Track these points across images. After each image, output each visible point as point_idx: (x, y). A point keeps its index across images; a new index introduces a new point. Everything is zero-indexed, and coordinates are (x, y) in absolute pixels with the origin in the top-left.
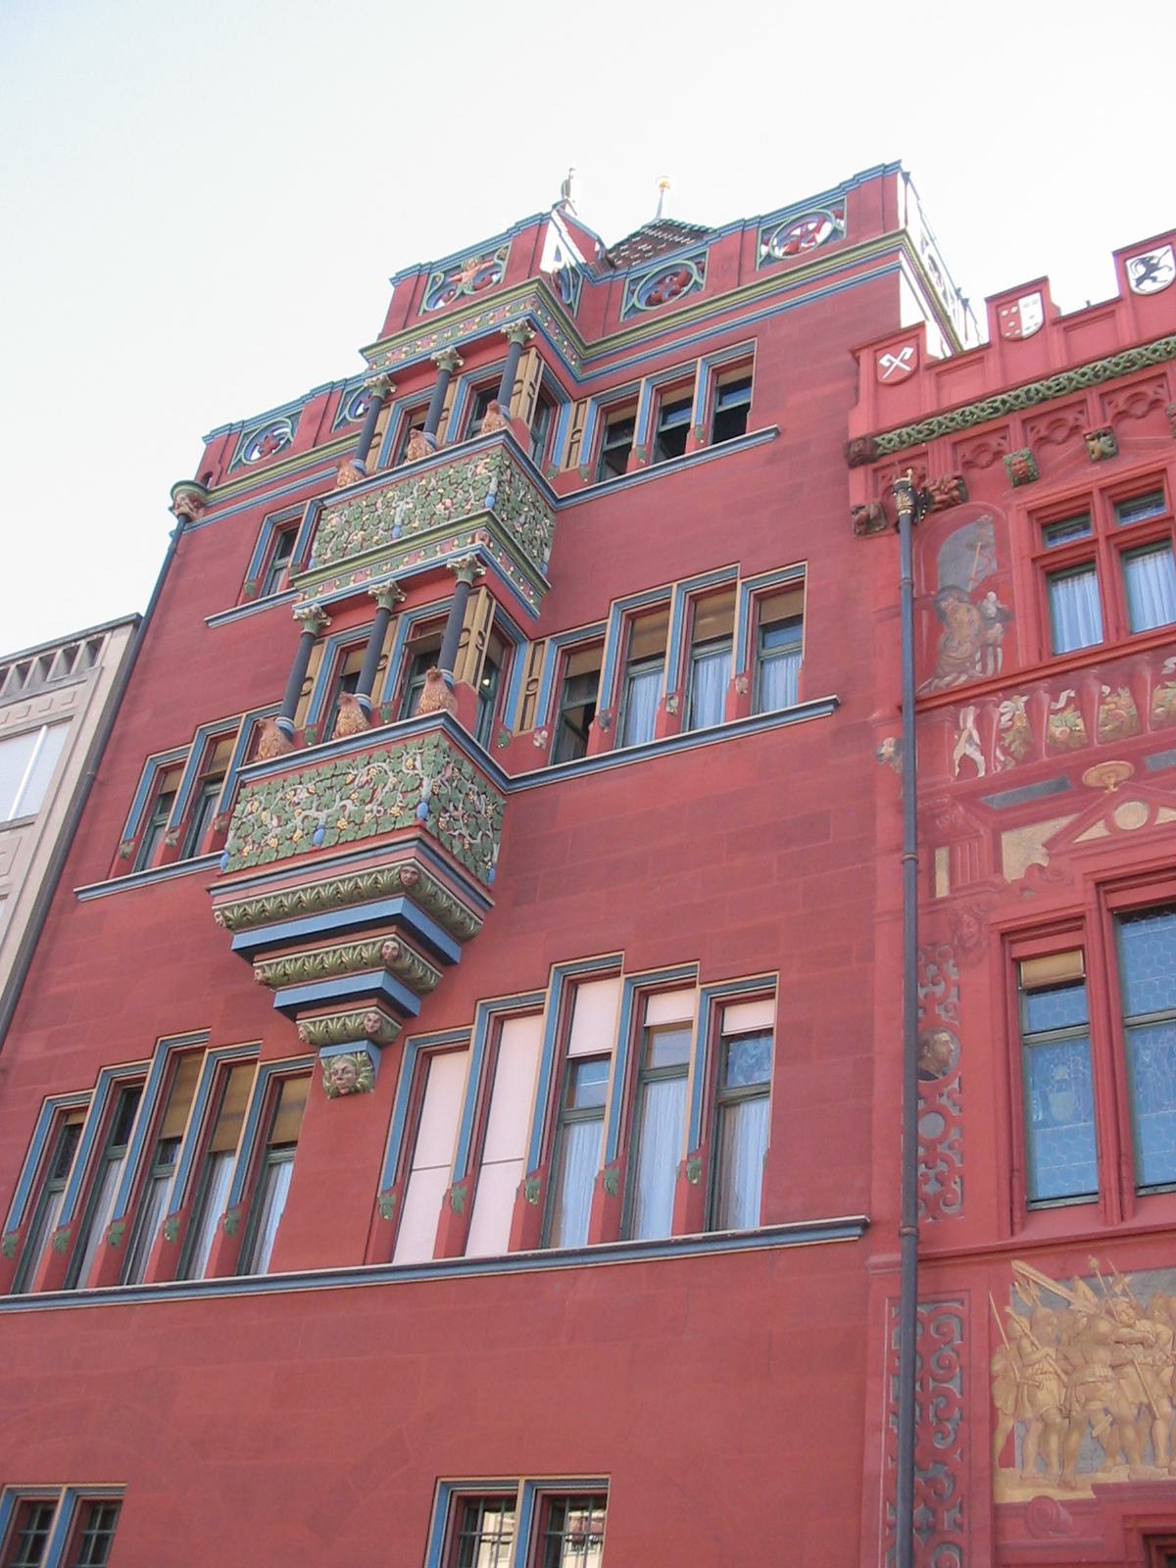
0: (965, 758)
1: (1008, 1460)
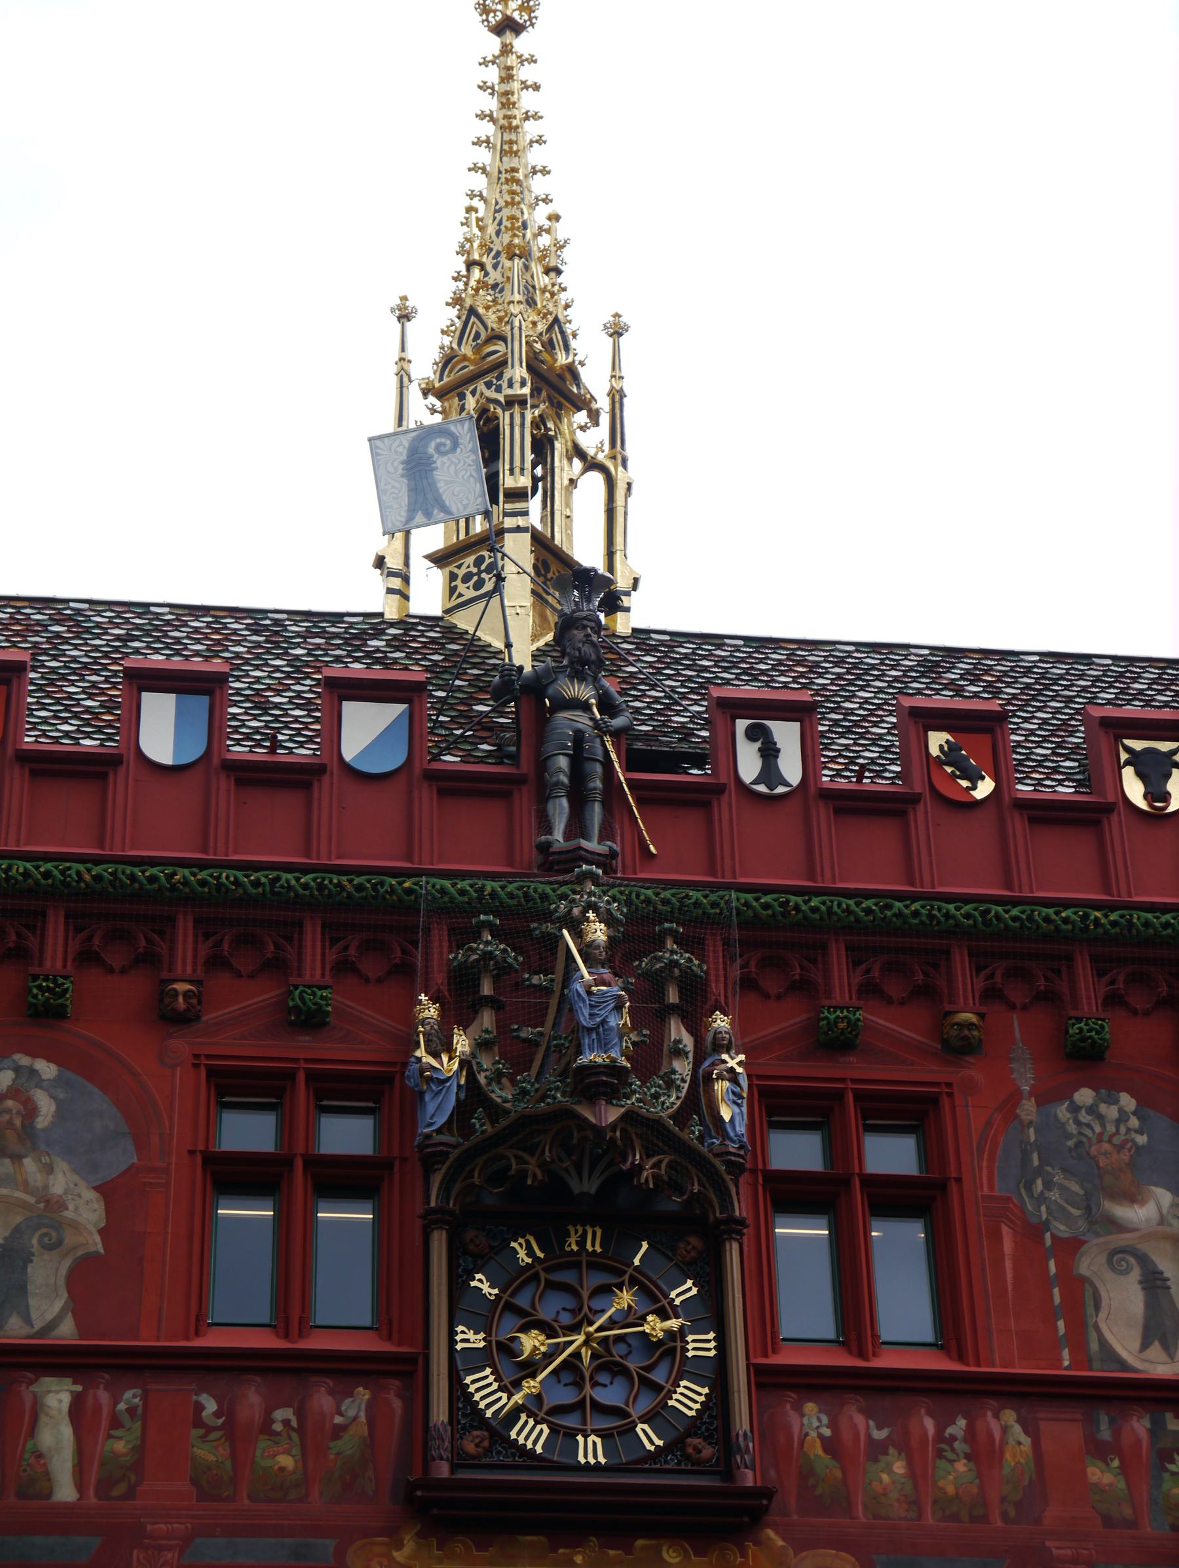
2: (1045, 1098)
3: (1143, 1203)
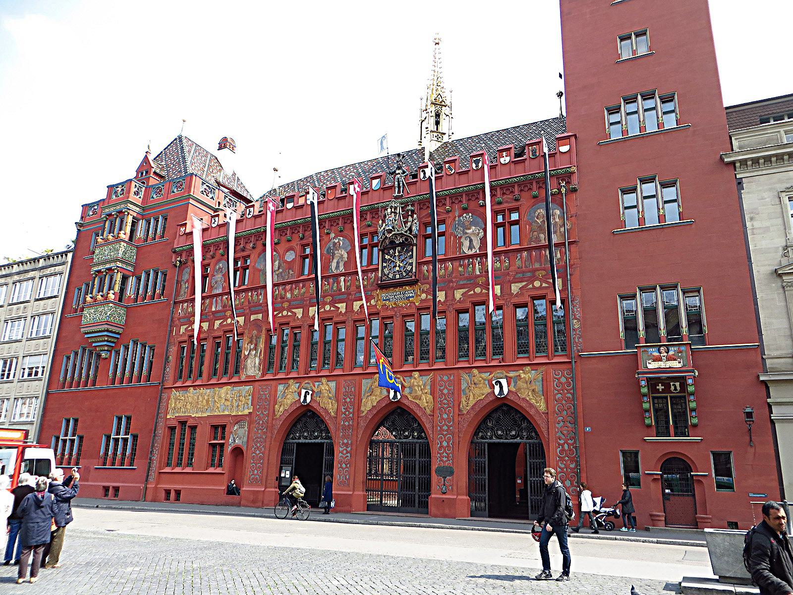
2: (459, 217)
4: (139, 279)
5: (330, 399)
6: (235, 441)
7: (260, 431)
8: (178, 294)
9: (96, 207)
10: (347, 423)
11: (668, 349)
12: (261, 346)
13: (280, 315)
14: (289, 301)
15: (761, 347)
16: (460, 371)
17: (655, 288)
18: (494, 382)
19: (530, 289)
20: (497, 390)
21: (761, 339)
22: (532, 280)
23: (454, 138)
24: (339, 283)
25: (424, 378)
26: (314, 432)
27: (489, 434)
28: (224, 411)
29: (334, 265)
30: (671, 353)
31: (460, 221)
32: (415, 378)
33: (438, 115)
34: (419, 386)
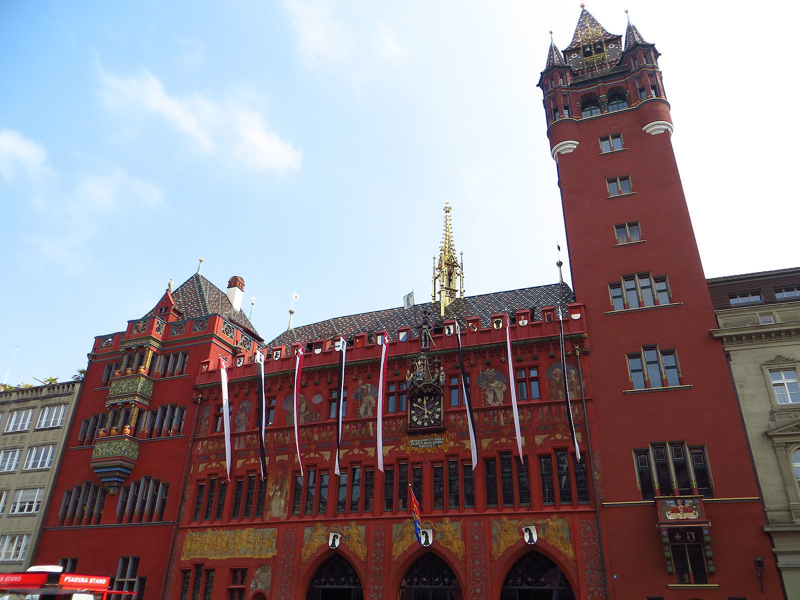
0: (199, 450)
1: (183, 555)
2: (484, 370)
3: (494, 383)
4: (154, 414)
5: (360, 542)
6: (257, 586)
7: (285, 576)
8: (197, 430)
9: (110, 340)
10: (377, 569)
11: (684, 502)
12: (288, 488)
13: (307, 457)
14: (315, 443)
15: (761, 501)
16: (490, 518)
17: (665, 445)
18: (523, 529)
19: (552, 441)
20: (527, 538)
21: (760, 493)
22: (553, 432)
23: (466, 295)
24: (367, 427)
25: (456, 524)
26: (341, 577)
27: (519, 581)
28: (245, 554)
29: (362, 410)
30: (687, 505)
31: (483, 375)
32: (447, 524)
33: (450, 274)
34: (450, 532)
